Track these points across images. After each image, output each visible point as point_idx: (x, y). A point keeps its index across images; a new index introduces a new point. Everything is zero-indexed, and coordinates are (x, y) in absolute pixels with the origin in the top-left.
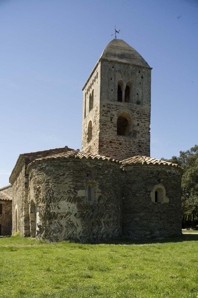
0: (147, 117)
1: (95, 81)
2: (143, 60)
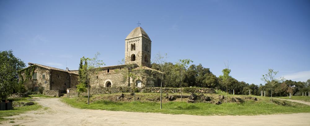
0: (150, 56)
2: (149, 38)
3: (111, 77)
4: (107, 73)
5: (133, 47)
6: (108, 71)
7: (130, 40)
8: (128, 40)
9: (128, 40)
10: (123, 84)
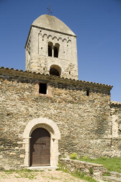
1: (63, 41)
3: (53, 111)
4: (36, 93)
5: (53, 50)
6: (43, 90)
7: (48, 33)
8: (39, 28)
9: (39, 28)
10: (98, 139)
